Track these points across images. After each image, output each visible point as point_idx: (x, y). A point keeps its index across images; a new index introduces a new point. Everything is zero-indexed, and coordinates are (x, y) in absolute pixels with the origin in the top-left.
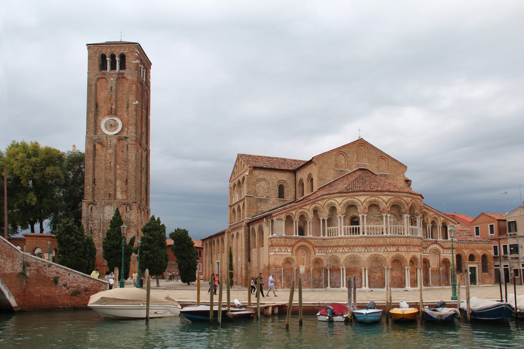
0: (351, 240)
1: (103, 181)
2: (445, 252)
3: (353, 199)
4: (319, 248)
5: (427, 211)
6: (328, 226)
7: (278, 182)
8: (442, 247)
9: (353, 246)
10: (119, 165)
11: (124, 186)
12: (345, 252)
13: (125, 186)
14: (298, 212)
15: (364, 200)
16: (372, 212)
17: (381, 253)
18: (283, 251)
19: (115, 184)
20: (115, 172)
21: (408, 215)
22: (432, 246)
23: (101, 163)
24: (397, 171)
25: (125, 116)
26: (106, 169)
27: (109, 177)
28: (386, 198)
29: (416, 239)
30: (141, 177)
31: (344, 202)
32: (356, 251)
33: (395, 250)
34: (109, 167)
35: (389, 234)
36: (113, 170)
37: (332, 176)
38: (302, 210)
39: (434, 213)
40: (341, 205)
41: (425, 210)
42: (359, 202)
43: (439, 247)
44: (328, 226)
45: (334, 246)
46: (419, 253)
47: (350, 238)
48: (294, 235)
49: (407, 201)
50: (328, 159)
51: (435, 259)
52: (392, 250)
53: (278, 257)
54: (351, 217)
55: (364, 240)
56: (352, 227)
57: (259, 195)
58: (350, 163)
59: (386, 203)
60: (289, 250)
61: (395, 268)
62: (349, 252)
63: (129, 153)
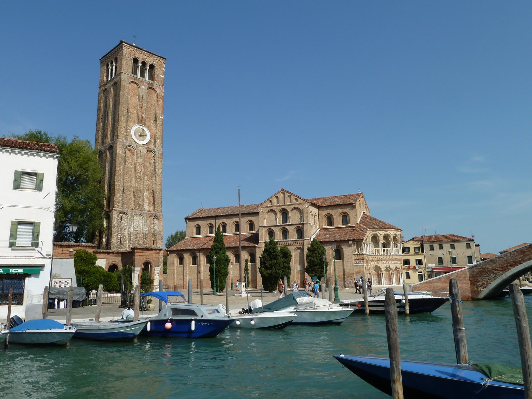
0: (387, 256)
1: (133, 190)
3: (387, 233)
10: (147, 175)
11: (150, 197)
12: (384, 264)
13: (151, 198)
17: (398, 265)
20: (144, 182)
23: (130, 171)
25: (152, 128)
26: (136, 178)
27: (139, 187)
31: (383, 233)
32: (389, 263)
36: (142, 181)
40: (382, 236)
42: (390, 234)
45: (377, 260)
47: (386, 255)
56: (384, 248)
62: (386, 264)
63: (157, 166)
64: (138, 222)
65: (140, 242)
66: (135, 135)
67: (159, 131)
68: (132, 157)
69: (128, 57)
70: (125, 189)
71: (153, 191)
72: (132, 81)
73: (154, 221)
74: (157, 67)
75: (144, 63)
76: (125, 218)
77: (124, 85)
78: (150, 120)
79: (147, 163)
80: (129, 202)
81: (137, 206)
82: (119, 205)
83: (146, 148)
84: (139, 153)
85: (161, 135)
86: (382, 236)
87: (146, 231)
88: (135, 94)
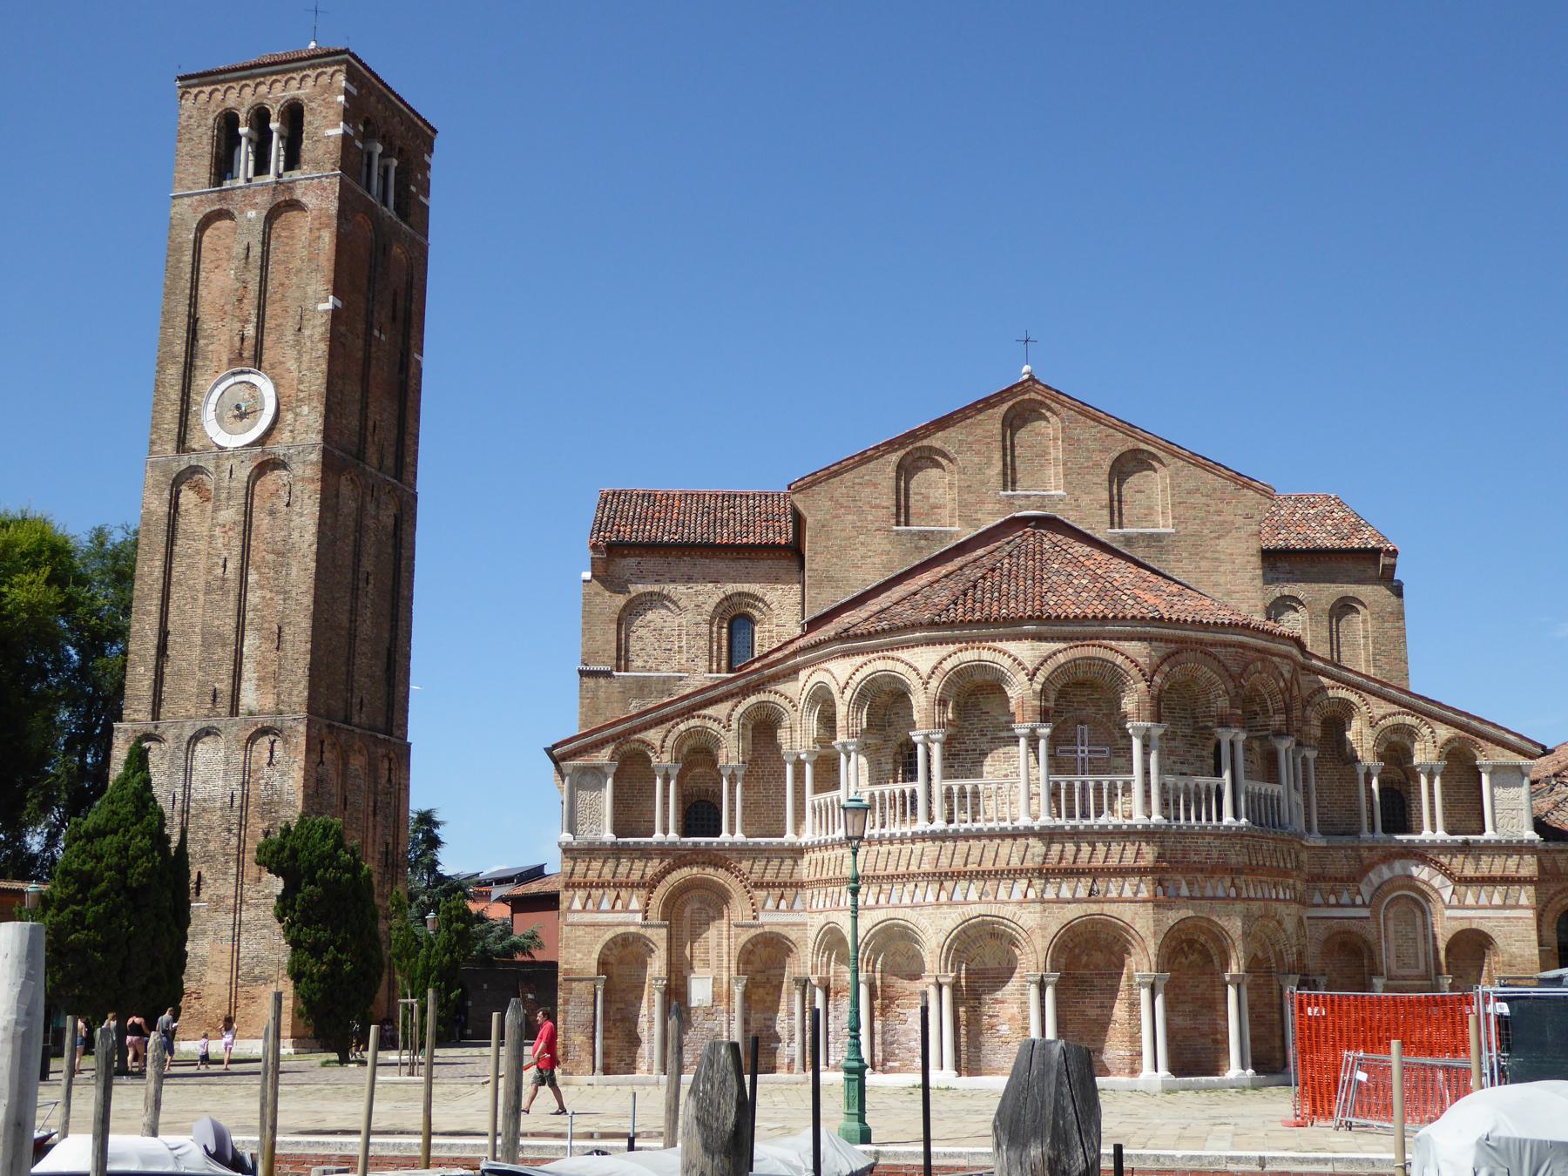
1: (198, 640)
2: (1470, 900)
3: (890, 665)
4: (778, 892)
5: (1354, 698)
6: (818, 789)
7: (726, 604)
8: (1450, 875)
9: (891, 878)
10: (258, 568)
13: (272, 656)
14: (675, 732)
15: (934, 663)
16: (984, 717)
17: (1007, 911)
18: (606, 905)
19: (239, 653)
21: (1149, 724)
22: (1391, 869)
23: (190, 567)
27: (217, 623)
28: (1027, 650)
30: (353, 612)
32: (906, 900)
33: (1082, 893)
34: (219, 583)
35: (1045, 820)
37: (877, 560)
38: (692, 723)
39: (1396, 708)
40: (848, 693)
41: (1343, 694)
44: (818, 789)
46: (1239, 906)
48: (658, 836)
49: (1141, 660)
50: (856, 488)
51: (1411, 936)
52: (1066, 893)
54: (901, 745)
55: (931, 848)
57: (639, 663)
58: (970, 498)
59: (1032, 676)
60: (635, 904)
61: (1097, 982)
63: (294, 518)
64: (207, 764)
65: (211, 847)
66: (220, 419)
67: (310, 369)
68: (202, 511)
69: (198, 127)
70: (170, 644)
71: (280, 628)
72: (208, 210)
73: (272, 752)
74: (313, 105)
75: (260, 117)
76: (158, 758)
77: (179, 240)
78: (282, 335)
79: (262, 515)
80: (183, 691)
81: (208, 699)
82: (140, 707)
83: (256, 457)
84: (226, 484)
85: (319, 381)
86: (848, 693)
87: (232, 796)
88: (224, 255)
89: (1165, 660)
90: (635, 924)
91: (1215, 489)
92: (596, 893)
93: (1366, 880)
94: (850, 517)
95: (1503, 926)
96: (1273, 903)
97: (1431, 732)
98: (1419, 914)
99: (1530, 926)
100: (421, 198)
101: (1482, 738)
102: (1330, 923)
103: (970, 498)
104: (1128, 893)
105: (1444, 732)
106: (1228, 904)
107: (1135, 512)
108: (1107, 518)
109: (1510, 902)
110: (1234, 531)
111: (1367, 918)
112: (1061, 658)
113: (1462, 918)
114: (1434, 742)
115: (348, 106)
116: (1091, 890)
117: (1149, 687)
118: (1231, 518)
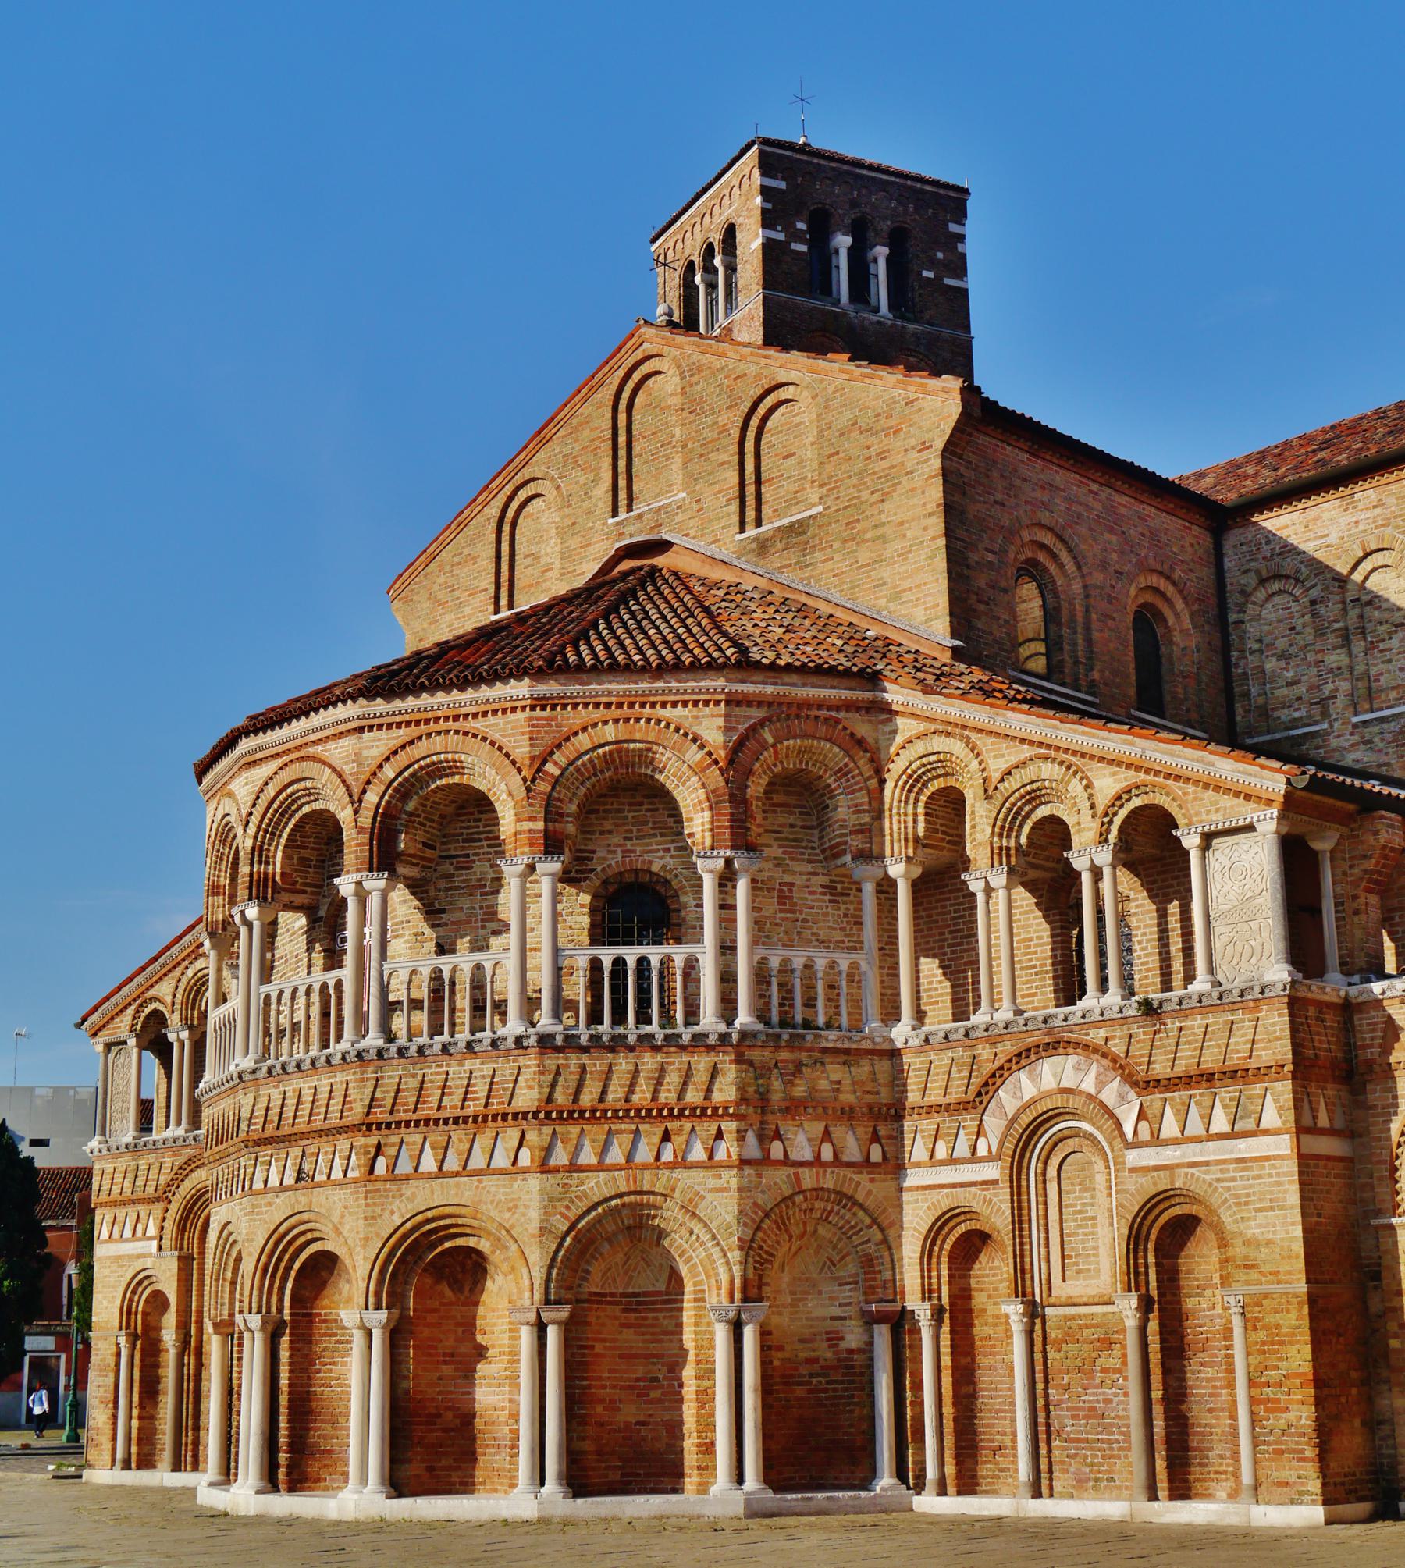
2: (1170, 1127)
5: (957, 747)
14: (184, 980)
22: (1034, 1078)
24: (882, 456)
29: (468, 1065)
33: (289, 1180)
39: (1026, 751)
43: (1101, 1084)
53: (106, 1272)
60: (152, 1231)
89: (387, 759)
90: (150, 1255)
91: (878, 415)
92: (120, 1212)
93: (992, 1104)
94: (449, 617)
95: (1233, 1179)
96: (664, 1174)
97: (1087, 787)
98: (1099, 1165)
99: (1285, 1174)
100: (948, 281)
101: (1178, 778)
102: (934, 1195)
103: (574, 542)
104: (337, 1174)
105: (1108, 783)
106: (516, 1180)
107: (783, 491)
108: (736, 519)
109: (1249, 1124)
110: (904, 480)
111: (995, 1182)
112: (271, 791)
113: (1157, 1168)
114: (1092, 807)
115: (769, 206)
116: (299, 1171)
117: (356, 812)
118: (896, 459)
